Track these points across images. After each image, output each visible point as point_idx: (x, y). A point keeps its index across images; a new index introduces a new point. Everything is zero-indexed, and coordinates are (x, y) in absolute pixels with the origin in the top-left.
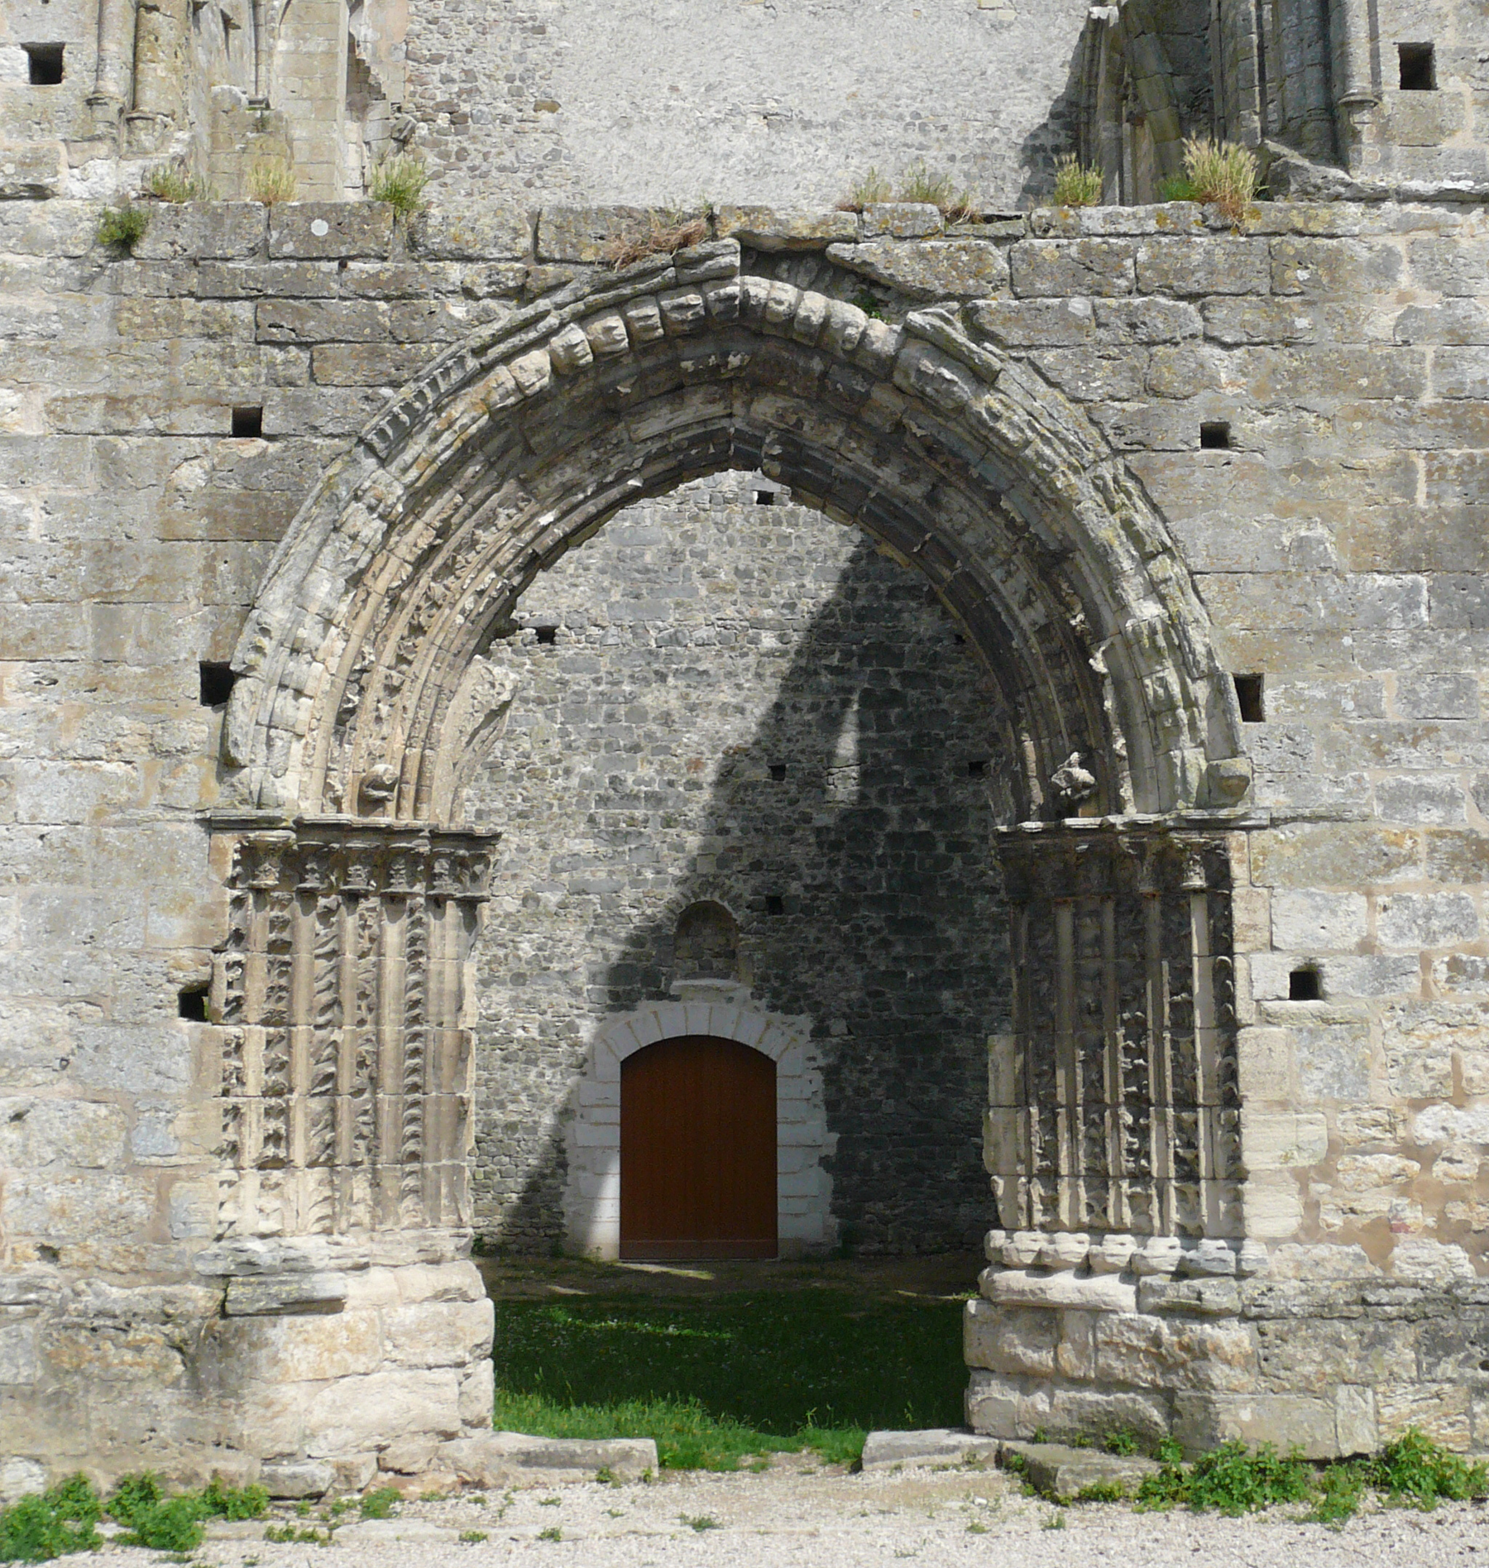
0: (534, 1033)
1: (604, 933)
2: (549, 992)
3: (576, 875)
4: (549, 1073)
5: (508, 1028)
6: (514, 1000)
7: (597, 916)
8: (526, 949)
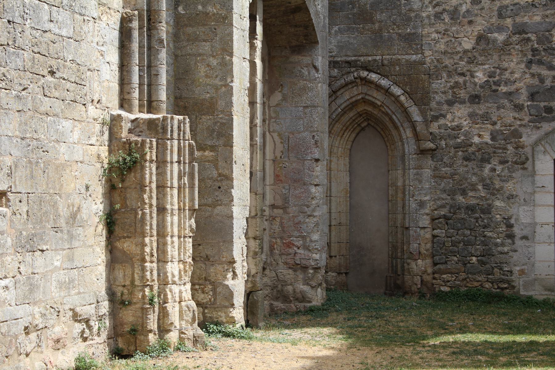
0: (487, 138)
1: (540, 63)
2: (498, 108)
3: (518, 20)
4: (499, 168)
5: (466, 134)
6: (471, 115)
7: (534, 50)
8: (480, 76)
